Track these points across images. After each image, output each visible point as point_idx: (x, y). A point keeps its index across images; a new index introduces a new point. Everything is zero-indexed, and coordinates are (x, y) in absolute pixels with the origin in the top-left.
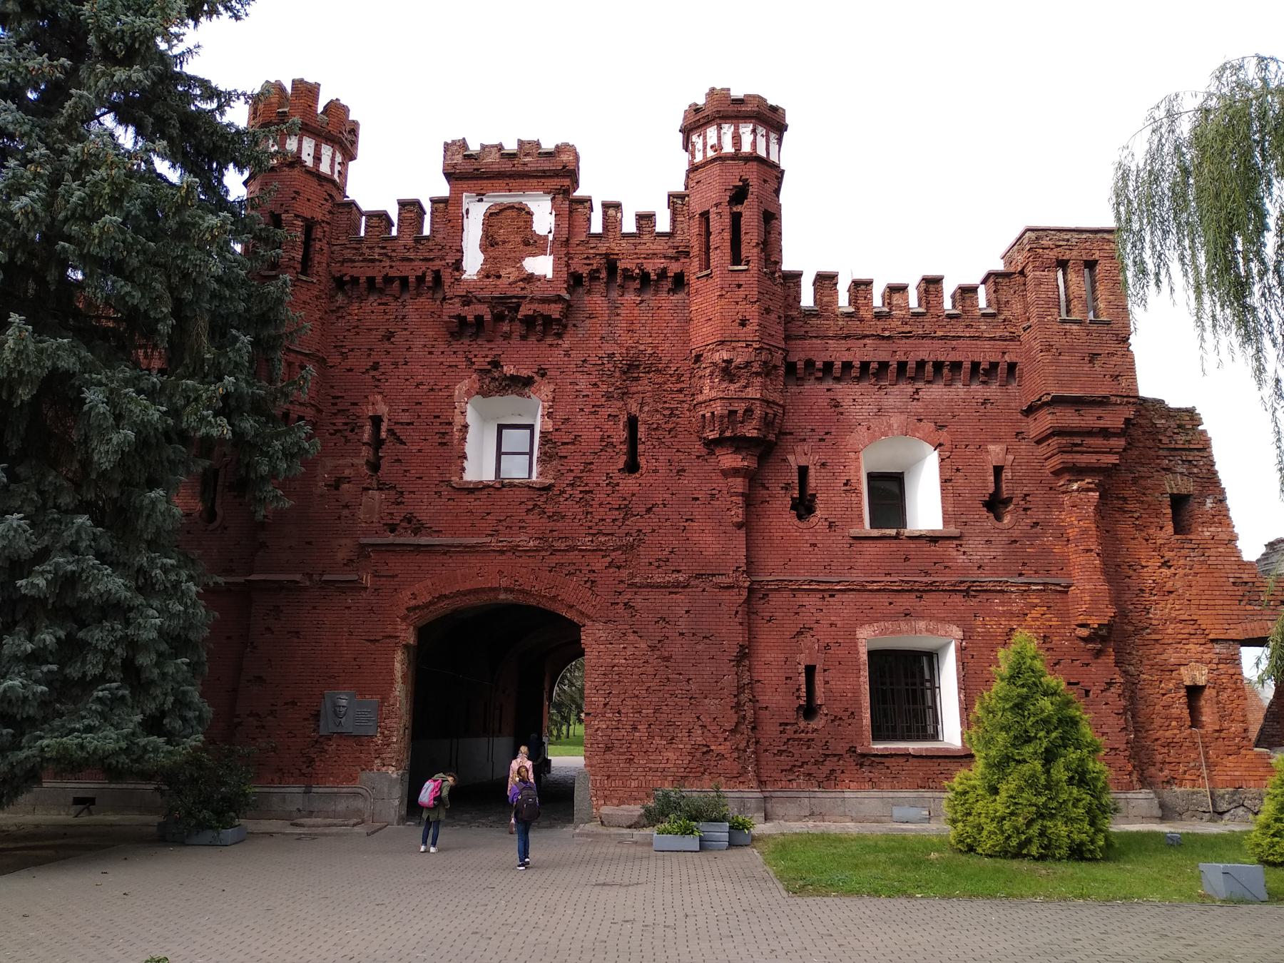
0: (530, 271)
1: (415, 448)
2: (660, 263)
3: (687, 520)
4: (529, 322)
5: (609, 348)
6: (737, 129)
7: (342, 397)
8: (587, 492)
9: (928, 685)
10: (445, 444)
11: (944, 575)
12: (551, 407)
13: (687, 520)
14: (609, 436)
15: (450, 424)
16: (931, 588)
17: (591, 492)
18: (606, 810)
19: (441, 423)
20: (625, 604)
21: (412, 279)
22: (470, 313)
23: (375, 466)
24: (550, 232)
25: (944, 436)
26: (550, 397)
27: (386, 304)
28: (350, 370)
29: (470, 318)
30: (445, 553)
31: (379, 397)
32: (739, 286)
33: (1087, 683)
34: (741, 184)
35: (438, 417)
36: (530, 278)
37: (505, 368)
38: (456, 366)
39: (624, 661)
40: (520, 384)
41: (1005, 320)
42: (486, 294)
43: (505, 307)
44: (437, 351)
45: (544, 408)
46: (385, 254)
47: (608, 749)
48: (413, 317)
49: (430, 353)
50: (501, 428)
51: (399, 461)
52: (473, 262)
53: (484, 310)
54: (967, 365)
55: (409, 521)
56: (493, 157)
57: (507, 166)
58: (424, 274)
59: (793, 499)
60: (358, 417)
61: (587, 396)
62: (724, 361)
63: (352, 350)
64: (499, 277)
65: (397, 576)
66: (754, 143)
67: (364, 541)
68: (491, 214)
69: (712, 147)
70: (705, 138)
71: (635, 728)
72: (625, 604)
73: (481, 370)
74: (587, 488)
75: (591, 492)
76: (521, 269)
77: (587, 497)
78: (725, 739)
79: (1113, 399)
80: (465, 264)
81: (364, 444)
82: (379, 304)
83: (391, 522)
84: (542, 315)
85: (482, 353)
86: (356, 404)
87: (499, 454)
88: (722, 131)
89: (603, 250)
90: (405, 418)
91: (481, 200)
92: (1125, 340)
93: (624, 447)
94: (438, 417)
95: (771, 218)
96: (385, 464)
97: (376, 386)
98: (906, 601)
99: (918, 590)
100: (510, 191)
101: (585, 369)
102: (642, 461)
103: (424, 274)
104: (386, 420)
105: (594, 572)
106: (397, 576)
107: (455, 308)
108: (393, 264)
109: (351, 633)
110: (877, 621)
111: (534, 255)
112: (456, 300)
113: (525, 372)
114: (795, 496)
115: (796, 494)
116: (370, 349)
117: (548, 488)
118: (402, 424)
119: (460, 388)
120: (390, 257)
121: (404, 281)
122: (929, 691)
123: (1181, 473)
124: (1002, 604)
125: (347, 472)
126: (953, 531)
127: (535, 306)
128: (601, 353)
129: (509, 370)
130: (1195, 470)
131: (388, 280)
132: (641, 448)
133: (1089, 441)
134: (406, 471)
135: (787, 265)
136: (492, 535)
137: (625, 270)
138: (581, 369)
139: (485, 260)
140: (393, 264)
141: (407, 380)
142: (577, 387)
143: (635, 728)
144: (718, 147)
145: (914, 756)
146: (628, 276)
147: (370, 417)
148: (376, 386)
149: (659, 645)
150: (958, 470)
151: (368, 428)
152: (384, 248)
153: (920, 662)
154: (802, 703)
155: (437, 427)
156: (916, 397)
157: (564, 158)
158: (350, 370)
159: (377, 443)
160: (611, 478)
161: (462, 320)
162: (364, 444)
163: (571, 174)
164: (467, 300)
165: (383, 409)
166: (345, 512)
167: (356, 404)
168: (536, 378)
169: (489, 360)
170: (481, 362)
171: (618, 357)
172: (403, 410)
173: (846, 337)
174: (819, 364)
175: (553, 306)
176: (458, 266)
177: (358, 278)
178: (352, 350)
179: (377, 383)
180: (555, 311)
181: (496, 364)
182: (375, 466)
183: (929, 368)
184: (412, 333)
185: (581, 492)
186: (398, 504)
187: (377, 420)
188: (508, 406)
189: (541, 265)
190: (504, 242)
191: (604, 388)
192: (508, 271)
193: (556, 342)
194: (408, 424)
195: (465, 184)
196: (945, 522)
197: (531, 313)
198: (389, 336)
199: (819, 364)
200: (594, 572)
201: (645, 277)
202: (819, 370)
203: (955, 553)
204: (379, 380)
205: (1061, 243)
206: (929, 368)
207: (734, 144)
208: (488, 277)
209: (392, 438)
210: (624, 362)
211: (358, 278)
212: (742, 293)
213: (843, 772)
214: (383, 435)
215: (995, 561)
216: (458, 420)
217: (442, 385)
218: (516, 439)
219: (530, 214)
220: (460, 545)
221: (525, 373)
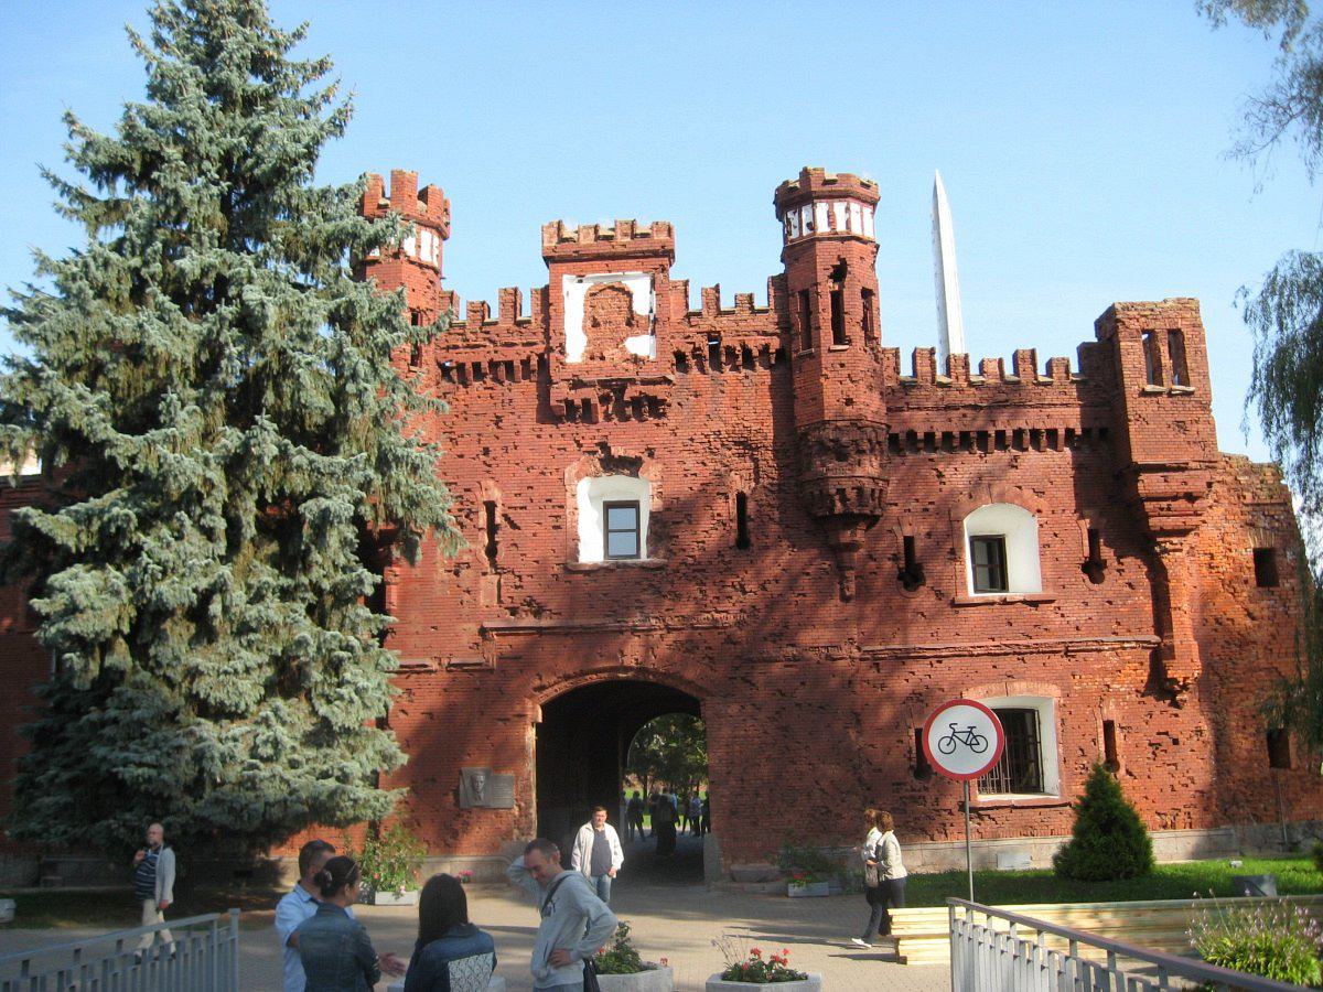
0: (633, 352)
1: (529, 533)
2: (762, 340)
3: (799, 595)
4: (636, 402)
5: (715, 426)
6: (831, 207)
7: (456, 483)
8: (699, 571)
9: (1030, 740)
10: (558, 527)
11: (1044, 637)
12: (661, 486)
13: (799, 595)
14: (719, 515)
15: (562, 507)
16: (1038, 651)
17: (704, 570)
18: (735, 867)
19: (553, 507)
20: (743, 679)
21: (517, 363)
22: (577, 397)
23: (492, 551)
24: (651, 311)
25: (1042, 503)
26: (659, 477)
27: (492, 388)
28: (461, 456)
29: (578, 402)
30: (566, 635)
31: (491, 483)
32: (842, 365)
33: (1174, 733)
34: (838, 263)
35: (550, 501)
36: (636, 360)
37: (613, 450)
38: (565, 449)
39: (743, 732)
40: (631, 466)
41: (1096, 386)
42: (592, 378)
43: (614, 389)
44: (545, 435)
45: (653, 489)
46: (491, 341)
47: (734, 813)
48: (518, 399)
49: (539, 437)
50: (608, 506)
51: (515, 545)
52: (576, 346)
53: (593, 394)
54: (1061, 432)
55: (529, 604)
56: (587, 241)
57: (605, 248)
58: (529, 358)
59: (900, 569)
60: (472, 503)
61: (695, 475)
62: (831, 441)
63: (462, 436)
64: (602, 358)
65: (520, 658)
66: (848, 223)
67: (487, 624)
68: (592, 295)
69: (809, 225)
70: (800, 216)
71: (757, 795)
72: (743, 679)
73: (588, 452)
74: (699, 567)
75: (704, 570)
76: (623, 350)
77: (699, 575)
78: (843, 801)
79: (1193, 465)
80: (568, 348)
81: (480, 529)
82: (485, 388)
83: (511, 605)
84: (647, 396)
85: (589, 434)
86: (468, 490)
87: (607, 531)
88: (817, 210)
89: (705, 328)
90: (518, 502)
91: (581, 281)
92: (1206, 407)
93: (734, 525)
94: (550, 501)
95: (867, 294)
96: (501, 548)
97: (488, 472)
98: (1010, 663)
99: (1020, 654)
100: (610, 271)
101: (692, 448)
102: (753, 539)
103: (529, 358)
104: (499, 505)
105: (710, 648)
106: (520, 658)
107: (560, 392)
108: (497, 349)
109: (482, 714)
110: (981, 683)
111: (637, 335)
112: (565, 384)
113: (633, 452)
114: (901, 566)
115: (902, 564)
116: (479, 435)
117: (660, 568)
118: (515, 508)
119: (570, 471)
120: (493, 342)
121: (509, 365)
122: (1031, 747)
123: (1264, 528)
124: (1097, 661)
125: (466, 558)
126: (1050, 594)
127: (641, 388)
128: (707, 432)
129: (617, 451)
130: (1277, 524)
131: (493, 365)
132: (750, 525)
133: (1174, 504)
134: (522, 555)
135: (887, 341)
136: (608, 616)
137: (728, 348)
138: (688, 448)
139: (589, 341)
140: (497, 349)
141: (517, 464)
142: (684, 466)
143: (757, 795)
144: (811, 226)
145: (1016, 808)
146: (730, 351)
147: (485, 503)
148: (488, 472)
149: (776, 716)
150: (1056, 535)
151: (483, 515)
152: (488, 333)
153: (1023, 716)
154: (912, 763)
155: (550, 511)
156: (1015, 464)
157: (663, 237)
158: (461, 456)
159: (492, 529)
160: (723, 556)
161: (569, 403)
162: (480, 529)
163: (668, 254)
164: (577, 384)
165: (496, 494)
166: (466, 597)
167: (468, 490)
168: (645, 457)
169: (596, 441)
170: (588, 444)
171: (724, 435)
172: (516, 495)
173: (947, 408)
174: (920, 436)
175: (658, 387)
176: (563, 352)
177: (464, 365)
178: (462, 436)
179: (488, 468)
180: (659, 391)
181: (604, 446)
182: (492, 551)
183: (1027, 437)
184: (519, 417)
185: (694, 571)
186: (516, 587)
187: (490, 507)
188: (620, 486)
189: (642, 345)
190: (605, 323)
191: (711, 466)
192: (611, 352)
193: (660, 421)
194: (521, 508)
195: (564, 266)
196: (1045, 585)
197: (637, 395)
198: (498, 420)
199: (920, 436)
200: (710, 648)
201: (747, 352)
202: (920, 441)
203: (1053, 616)
204: (490, 466)
205: (1146, 313)
206: (1027, 437)
207: (830, 224)
208: (592, 358)
209: (505, 523)
210: (730, 439)
211: (464, 365)
212: (845, 372)
213: (952, 825)
214: (499, 519)
215: (1090, 621)
216: (570, 502)
217: (552, 468)
218: (622, 518)
219: (629, 294)
220: (582, 627)
221: (632, 454)
